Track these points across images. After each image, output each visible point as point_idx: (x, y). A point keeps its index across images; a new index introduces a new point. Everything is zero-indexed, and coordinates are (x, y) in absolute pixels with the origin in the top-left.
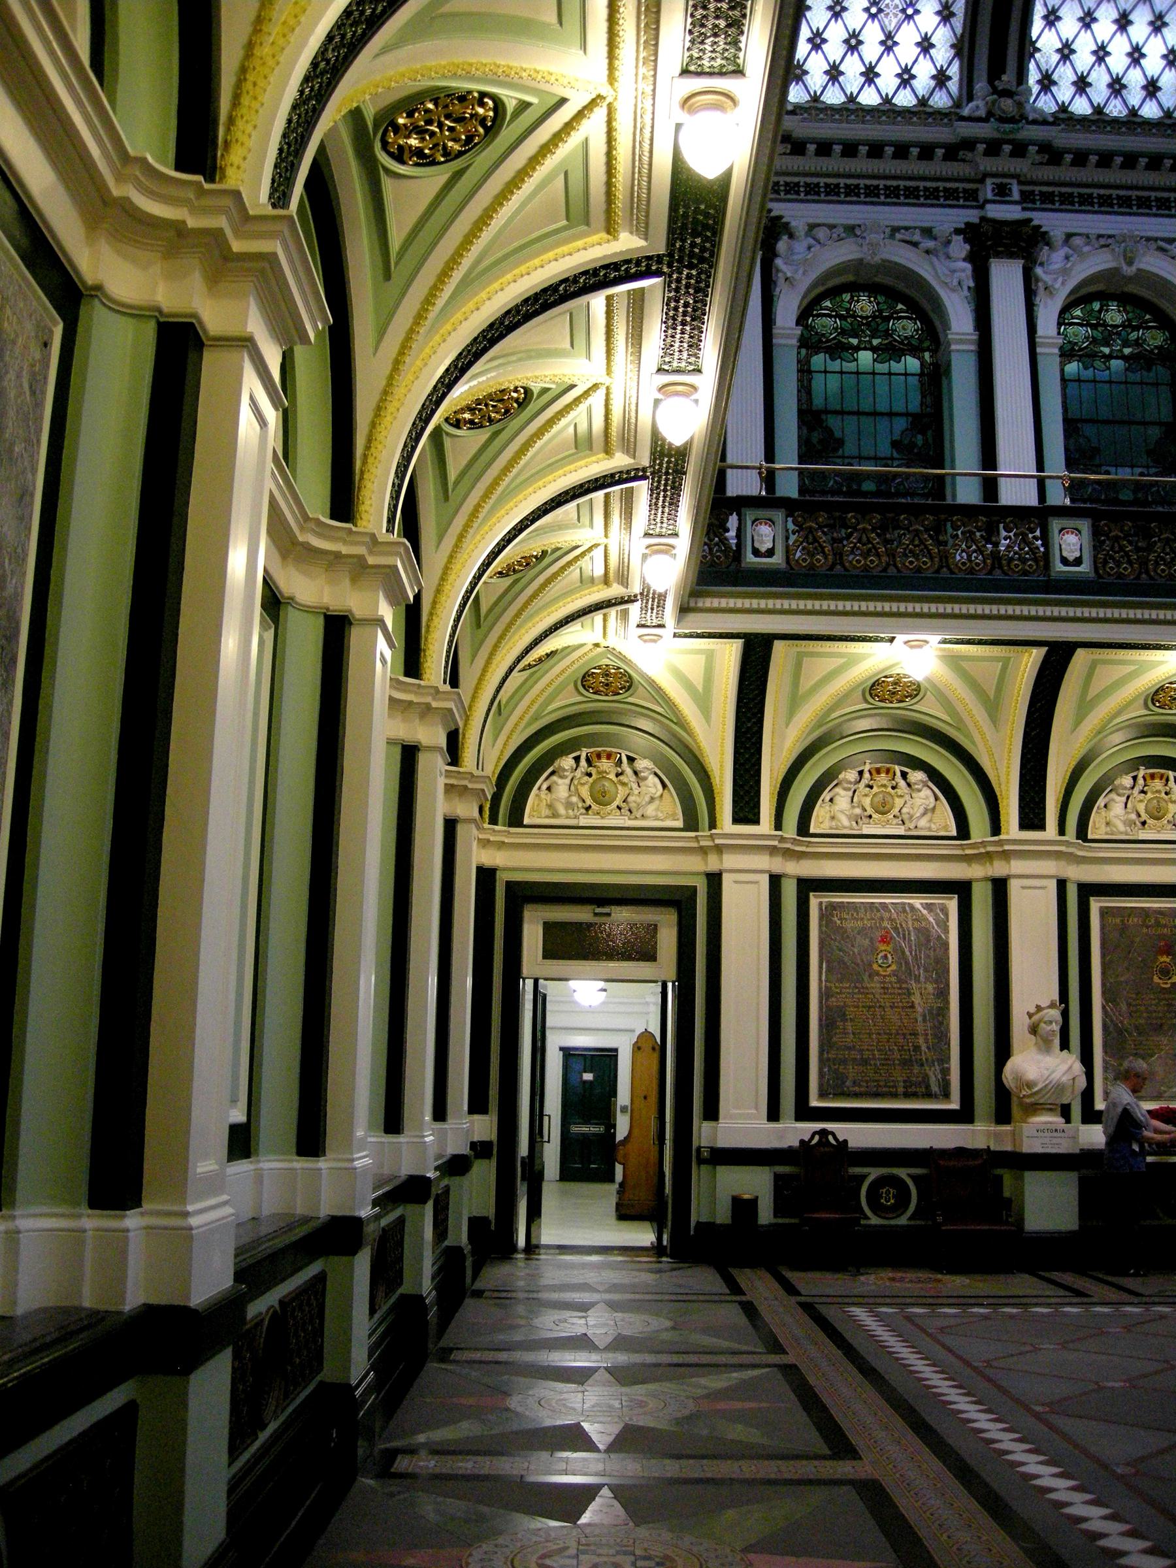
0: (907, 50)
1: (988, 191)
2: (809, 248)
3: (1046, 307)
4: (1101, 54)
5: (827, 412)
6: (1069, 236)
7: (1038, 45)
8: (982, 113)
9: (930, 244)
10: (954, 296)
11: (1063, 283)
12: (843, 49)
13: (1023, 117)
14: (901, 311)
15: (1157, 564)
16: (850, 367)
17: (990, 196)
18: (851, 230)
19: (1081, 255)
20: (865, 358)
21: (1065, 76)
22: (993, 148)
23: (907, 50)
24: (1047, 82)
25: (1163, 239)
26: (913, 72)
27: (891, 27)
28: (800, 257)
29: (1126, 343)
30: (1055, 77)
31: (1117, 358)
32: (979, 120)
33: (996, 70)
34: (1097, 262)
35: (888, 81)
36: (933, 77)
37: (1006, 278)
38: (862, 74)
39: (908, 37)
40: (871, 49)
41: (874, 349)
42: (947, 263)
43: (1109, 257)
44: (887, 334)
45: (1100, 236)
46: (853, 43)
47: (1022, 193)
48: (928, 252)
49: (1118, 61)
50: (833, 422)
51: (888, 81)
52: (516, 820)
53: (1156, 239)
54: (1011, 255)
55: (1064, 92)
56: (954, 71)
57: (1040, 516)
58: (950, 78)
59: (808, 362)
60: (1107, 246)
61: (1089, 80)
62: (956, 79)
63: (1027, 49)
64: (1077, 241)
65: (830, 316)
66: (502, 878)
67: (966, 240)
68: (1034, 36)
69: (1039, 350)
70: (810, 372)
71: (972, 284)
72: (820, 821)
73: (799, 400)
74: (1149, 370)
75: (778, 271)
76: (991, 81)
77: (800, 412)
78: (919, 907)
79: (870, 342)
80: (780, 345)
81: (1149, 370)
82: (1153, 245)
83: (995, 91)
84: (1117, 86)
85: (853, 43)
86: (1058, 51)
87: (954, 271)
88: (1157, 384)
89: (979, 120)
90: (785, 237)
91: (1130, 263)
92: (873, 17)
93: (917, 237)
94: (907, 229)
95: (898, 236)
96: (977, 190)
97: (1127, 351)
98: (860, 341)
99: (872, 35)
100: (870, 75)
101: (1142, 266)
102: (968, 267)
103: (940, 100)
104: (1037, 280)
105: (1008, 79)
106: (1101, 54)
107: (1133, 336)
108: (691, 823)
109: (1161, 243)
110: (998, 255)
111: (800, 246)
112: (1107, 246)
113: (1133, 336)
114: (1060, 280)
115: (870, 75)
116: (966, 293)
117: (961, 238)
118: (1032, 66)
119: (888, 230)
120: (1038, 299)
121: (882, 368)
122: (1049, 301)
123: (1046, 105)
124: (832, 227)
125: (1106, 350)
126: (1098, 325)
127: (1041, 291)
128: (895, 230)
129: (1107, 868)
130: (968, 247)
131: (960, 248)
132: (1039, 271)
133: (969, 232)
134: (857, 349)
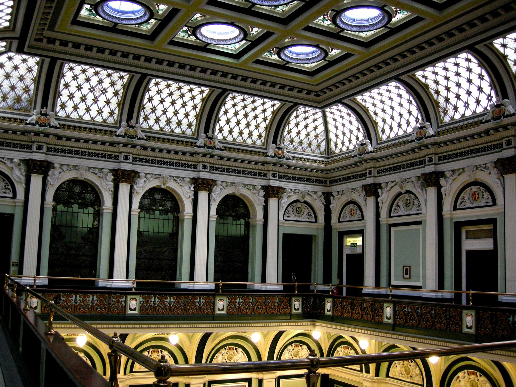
0: (101, 103)
1: (122, 158)
2: (60, 173)
4: (165, 111)
5: (61, 226)
6: (146, 174)
7: (145, 106)
8: (123, 134)
9: (101, 175)
10: (107, 193)
11: (143, 190)
12: (80, 100)
13: (136, 136)
14: (89, 190)
15: (159, 309)
16: (70, 210)
17: (122, 160)
18: (75, 167)
19: (149, 181)
20: (76, 207)
21: (152, 117)
22: (125, 145)
23: (101, 103)
24: (146, 118)
25: (176, 177)
26: (103, 110)
28: (56, 176)
29: (160, 206)
30: (149, 117)
31: (157, 210)
32: (122, 136)
33: (130, 118)
34: (154, 183)
35: (94, 112)
36: (109, 113)
37: (124, 189)
39: (102, 99)
40: (89, 102)
41: (79, 204)
42: (105, 181)
43: (158, 182)
44: (83, 199)
45: (156, 175)
46: (84, 99)
47: (133, 158)
48: (100, 177)
49: (170, 114)
50: (63, 230)
51: (94, 112)
53: (174, 177)
54: (127, 182)
55: (151, 122)
56: (116, 111)
57: (125, 292)
58: (115, 114)
59: (56, 208)
61: (160, 119)
62: (117, 114)
63: (142, 107)
65: (65, 191)
67: (113, 175)
68: (144, 103)
69: (132, 213)
70: (56, 211)
71: (113, 190)
73: (52, 221)
74: (167, 215)
75: (48, 181)
76: (127, 122)
77: (52, 225)
79: (77, 201)
80: (47, 208)
81: (167, 215)
82: (172, 178)
83: (129, 126)
85: (84, 99)
86: (151, 109)
88: (169, 220)
89: (122, 136)
91: (164, 185)
92: (91, 91)
94: (94, 168)
95: (90, 170)
96: (118, 156)
97: (160, 208)
98: (74, 201)
102: (112, 184)
103: (111, 121)
104: (134, 189)
105: (133, 122)
106: (165, 111)
107: (163, 203)
110: (123, 182)
111: (57, 172)
113: (163, 203)
115: (88, 110)
116: (111, 193)
118: (142, 112)
119: (87, 168)
121: (81, 211)
124: (68, 165)
125: (154, 208)
126: (153, 199)
127: (135, 193)
128: (90, 168)
129: (139, 380)
130: (113, 177)
131: (110, 177)
132: (135, 186)
133: (115, 172)
134: (73, 203)
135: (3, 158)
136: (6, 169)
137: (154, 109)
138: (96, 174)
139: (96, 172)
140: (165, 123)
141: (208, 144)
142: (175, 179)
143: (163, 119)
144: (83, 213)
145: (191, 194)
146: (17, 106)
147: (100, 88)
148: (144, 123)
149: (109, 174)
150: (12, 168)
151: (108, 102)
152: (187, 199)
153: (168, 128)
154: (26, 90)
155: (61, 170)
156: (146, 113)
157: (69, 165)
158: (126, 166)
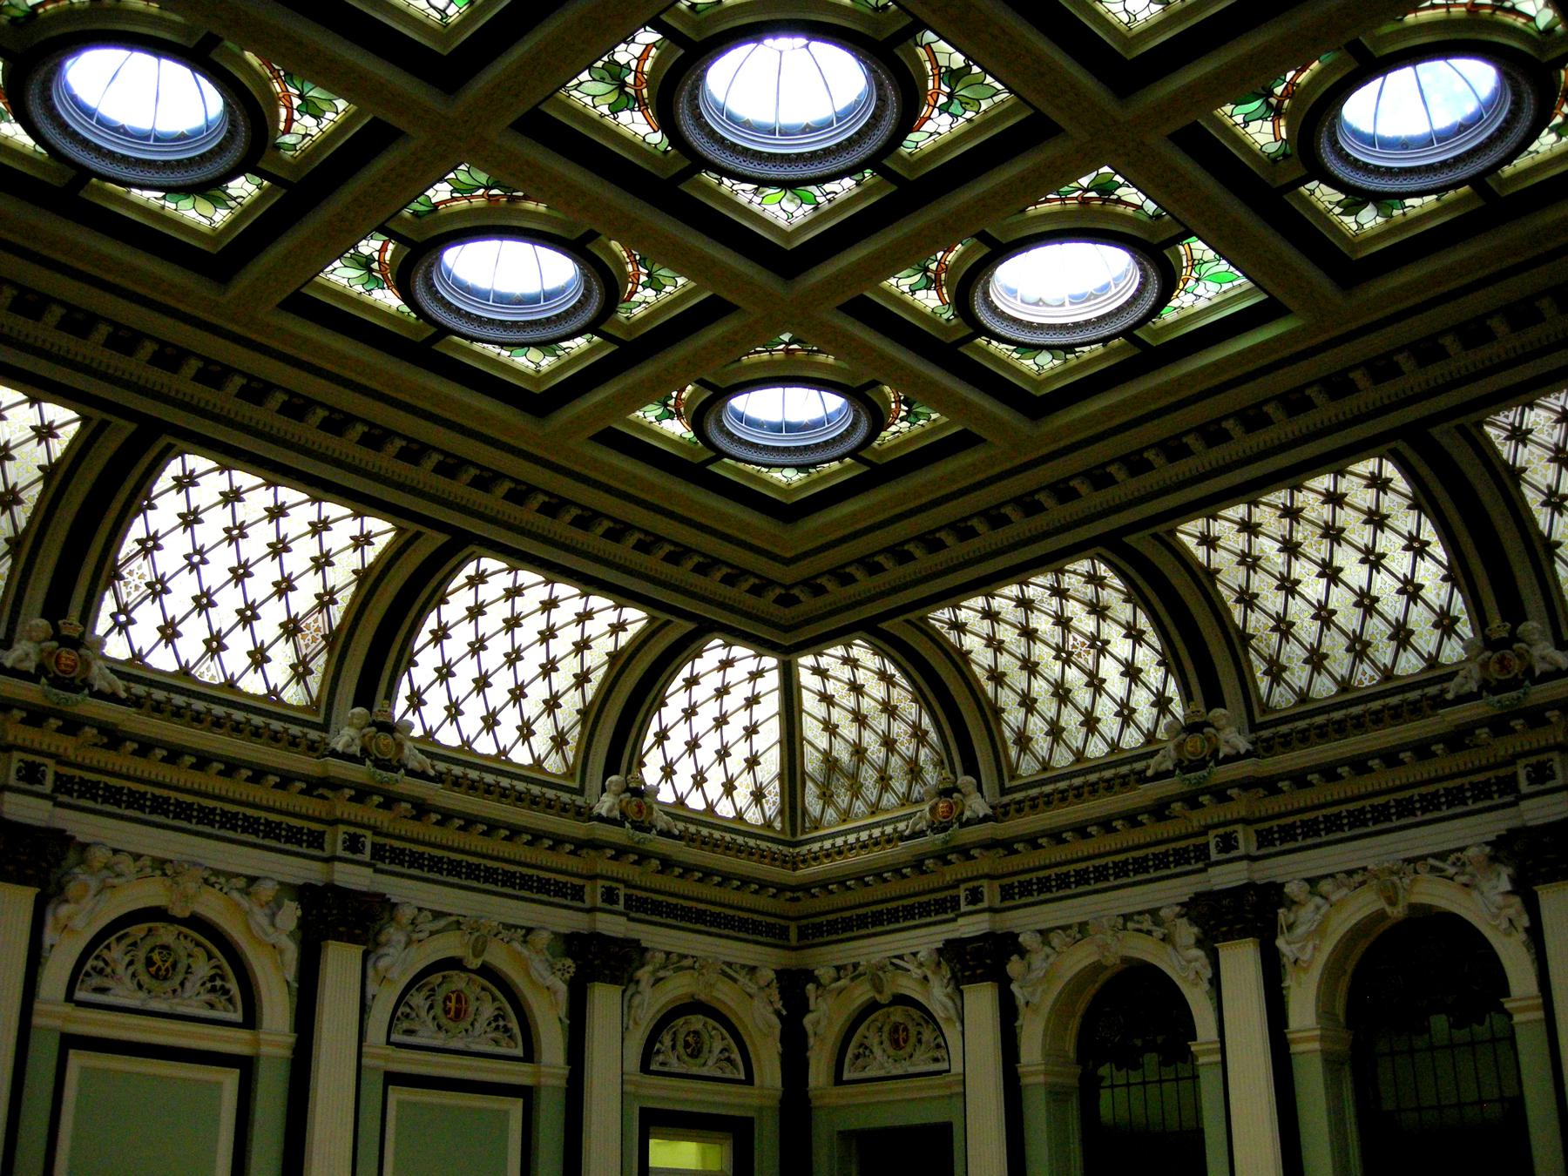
2: (1048, 956)
3: (1300, 984)
9: (1158, 932)
21: (1293, 654)
23: (1116, 684)
24: (1276, 671)
25: (1437, 856)
27: (1090, 665)
32: (1167, 774)
34: (1360, 906)
38: (1082, 724)
45: (1350, 873)
53: (1424, 858)
55: (1298, 675)
58: (1171, 700)
61: (1323, 650)
62: (1177, 698)
64: (1325, 886)
74: (1481, 1023)
81: (1481, 1023)
84: (1359, 647)
87: (1189, 962)
89: (1167, 774)
90: (1015, 958)
93: (1147, 925)
95: (1130, 925)
101: (1415, 899)
102: (1199, 953)
109: (1431, 861)
111: (1037, 961)
114: (1310, 946)
117: (1185, 920)
118: (1253, 656)
119: (1121, 920)
121: (1168, 1073)
123: (1282, 698)
124: (1064, 928)
128: (1127, 917)
130: (1195, 930)
131: (1187, 933)
132: (1280, 943)
135: (901, 957)
136: (911, 984)
137: (1283, 626)
140: (1347, 659)
141: (1495, 673)
142: (1439, 862)
143: (1335, 646)
145: (1511, 912)
146: (917, 790)
147: (1080, 639)
148: (1277, 691)
149: (1179, 921)
150: (925, 978)
152: (1508, 934)
153: (1369, 672)
154: (918, 734)
155: (1047, 950)
156: (1266, 652)
157: (1069, 927)
158: (1227, 876)
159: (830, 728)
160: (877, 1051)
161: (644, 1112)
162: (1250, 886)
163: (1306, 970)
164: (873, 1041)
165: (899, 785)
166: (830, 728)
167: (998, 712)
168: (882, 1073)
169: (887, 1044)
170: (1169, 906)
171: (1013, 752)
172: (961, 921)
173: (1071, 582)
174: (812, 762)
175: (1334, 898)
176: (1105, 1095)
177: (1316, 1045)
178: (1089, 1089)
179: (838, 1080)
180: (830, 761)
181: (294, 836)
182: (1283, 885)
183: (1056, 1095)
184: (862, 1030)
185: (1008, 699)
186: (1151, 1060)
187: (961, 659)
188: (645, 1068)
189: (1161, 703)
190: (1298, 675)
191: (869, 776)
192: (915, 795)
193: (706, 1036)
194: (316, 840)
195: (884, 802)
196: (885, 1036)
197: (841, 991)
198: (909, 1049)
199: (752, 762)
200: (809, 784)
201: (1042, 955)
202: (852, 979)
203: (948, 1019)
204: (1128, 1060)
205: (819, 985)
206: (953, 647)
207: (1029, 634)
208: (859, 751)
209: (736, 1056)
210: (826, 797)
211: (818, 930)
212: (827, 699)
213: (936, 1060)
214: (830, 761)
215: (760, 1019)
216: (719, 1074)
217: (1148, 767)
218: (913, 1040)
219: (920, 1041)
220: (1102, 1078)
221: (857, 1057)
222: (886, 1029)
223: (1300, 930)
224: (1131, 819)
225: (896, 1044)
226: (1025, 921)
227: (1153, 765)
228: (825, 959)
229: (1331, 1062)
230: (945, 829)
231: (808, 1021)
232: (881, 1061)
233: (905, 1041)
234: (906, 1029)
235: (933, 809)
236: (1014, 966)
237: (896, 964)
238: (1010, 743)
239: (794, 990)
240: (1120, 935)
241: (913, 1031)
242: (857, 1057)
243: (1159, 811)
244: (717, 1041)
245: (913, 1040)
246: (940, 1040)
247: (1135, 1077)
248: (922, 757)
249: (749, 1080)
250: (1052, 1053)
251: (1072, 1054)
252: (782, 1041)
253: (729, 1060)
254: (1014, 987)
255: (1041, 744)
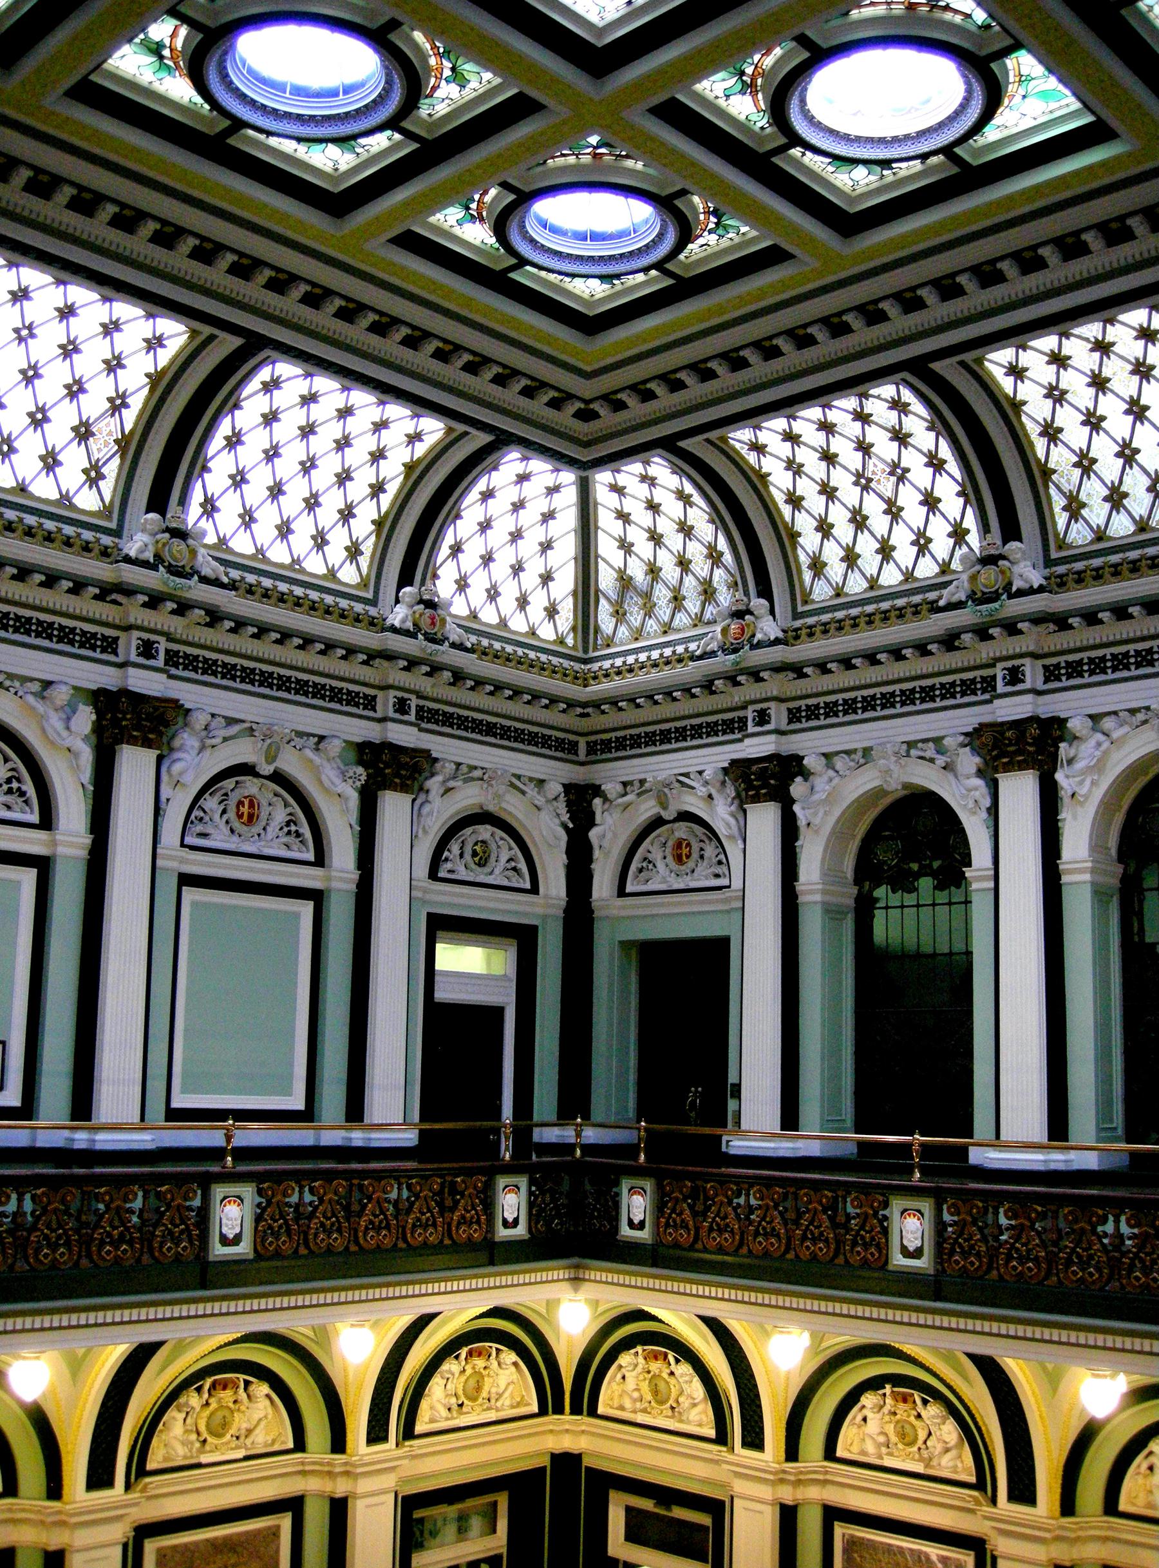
2: (831, 780)
3: (1075, 818)
9: (941, 761)
10: (974, 819)
11: (1093, 783)
12: (851, 528)
21: (1094, 492)
24: (1075, 507)
27: (889, 494)
32: (959, 605)
35: (905, 554)
36: (949, 535)
38: (877, 552)
40: (879, 522)
41: (933, 874)
43: (1152, 735)
45: (1133, 712)
46: (859, 521)
52: (593, 1412)
54: (1022, 766)
55: (1097, 512)
58: (967, 531)
60: (1145, 722)
61: (1124, 488)
64: (1108, 723)
66: (586, 1462)
72: (849, 1443)
78: (934, 1558)
79: (930, 866)
85: (859, 521)
87: (969, 790)
89: (959, 605)
90: (799, 779)
95: (913, 752)
99: (873, 507)
100: (886, 551)
102: (979, 782)
108: (722, 1438)
111: (822, 783)
112: (1145, 722)
114: (1088, 782)
115: (886, 551)
118: (1053, 491)
119: (905, 747)
120: (1065, 809)
121: (942, 897)
122: (1079, 810)
123: (1079, 535)
124: (848, 752)
128: (911, 745)
131: (969, 762)
132: (1059, 776)
134: (918, 875)
135: (687, 775)
137: (1086, 463)
138: (932, 760)
139: (928, 754)
144: (950, 904)
149: (962, 751)
150: (710, 796)
151: (930, 502)
154: (714, 556)
155: (831, 773)
156: (1066, 488)
157: (855, 751)
158: (1011, 708)
159: (626, 547)
160: (660, 865)
161: (431, 917)
162: (1034, 719)
163: (1082, 804)
164: (657, 855)
165: (693, 605)
166: (626, 547)
167: (794, 536)
168: (663, 887)
169: (670, 859)
170: (954, 735)
171: (807, 576)
172: (747, 741)
173: (877, 408)
174: (606, 580)
175: (1115, 735)
176: (879, 915)
177: (1087, 877)
178: (864, 909)
179: (622, 892)
180: (625, 581)
181: (88, 641)
182: (1066, 720)
183: (832, 912)
184: (646, 844)
185: (805, 524)
186: (925, 883)
187: (758, 481)
188: (433, 875)
189: (958, 534)
190: (1097, 512)
191: (662, 595)
192: (708, 616)
193: (493, 846)
194: (110, 645)
195: (676, 623)
196: (668, 850)
197: (626, 807)
198: (691, 864)
199: (547, 578)
200: (603, 602)
201: (825, 778)
202: (639, 795)
203: (730, 837)
204: (903, 882)
205: (606, 799)
206: (752, 468)
207: (829, 458)
208: (653, 571)
209: (523, 866)
210: (619, 614)
211: (606, 746)
212: (623, 517)
213: (717, 876)
214: (625, 581)
215: (547, 832)
216: (506, 883)
217: (940, 597)
218: (695, 855)
219: (702, 857)
220: (877, 900)
221: (641, 870)
222: (670, 844)
223: (1079, 765)
224: (922, 649)
225: (679, 859)
226: (809, 744)
227: (946, 596)
228: (611, 775)
229: (1099, 894)
230: (735, 651)
231: (593, 834)
232: (664, 875)
233: (688, 857)
234: (689, 845)
235: (725, 631)
236: (797, 788)
237: (682, 781)
238: (804, 567)
239: (581, 802)
240: (903, 761)
241: (695, 846)
242: (641, 870)
243: (950, 641)
244: (504, 851)
245: (695, 855)
246: (722, 857)
247: (910, 899)
248: (716, 578)
249: (534, 890)
250: (830, 873)
251: (850, 875)
252: (567, 853)
253: (514, 869)
254: (796, 808)
255: (835, 569)
